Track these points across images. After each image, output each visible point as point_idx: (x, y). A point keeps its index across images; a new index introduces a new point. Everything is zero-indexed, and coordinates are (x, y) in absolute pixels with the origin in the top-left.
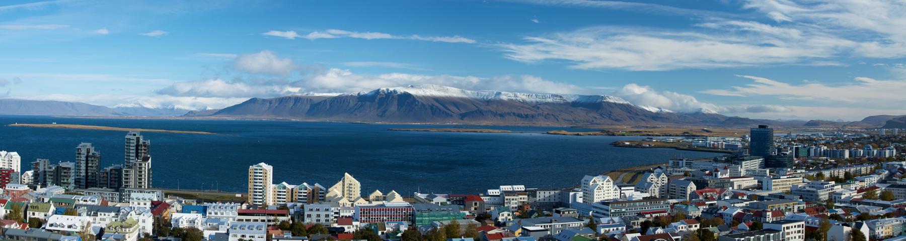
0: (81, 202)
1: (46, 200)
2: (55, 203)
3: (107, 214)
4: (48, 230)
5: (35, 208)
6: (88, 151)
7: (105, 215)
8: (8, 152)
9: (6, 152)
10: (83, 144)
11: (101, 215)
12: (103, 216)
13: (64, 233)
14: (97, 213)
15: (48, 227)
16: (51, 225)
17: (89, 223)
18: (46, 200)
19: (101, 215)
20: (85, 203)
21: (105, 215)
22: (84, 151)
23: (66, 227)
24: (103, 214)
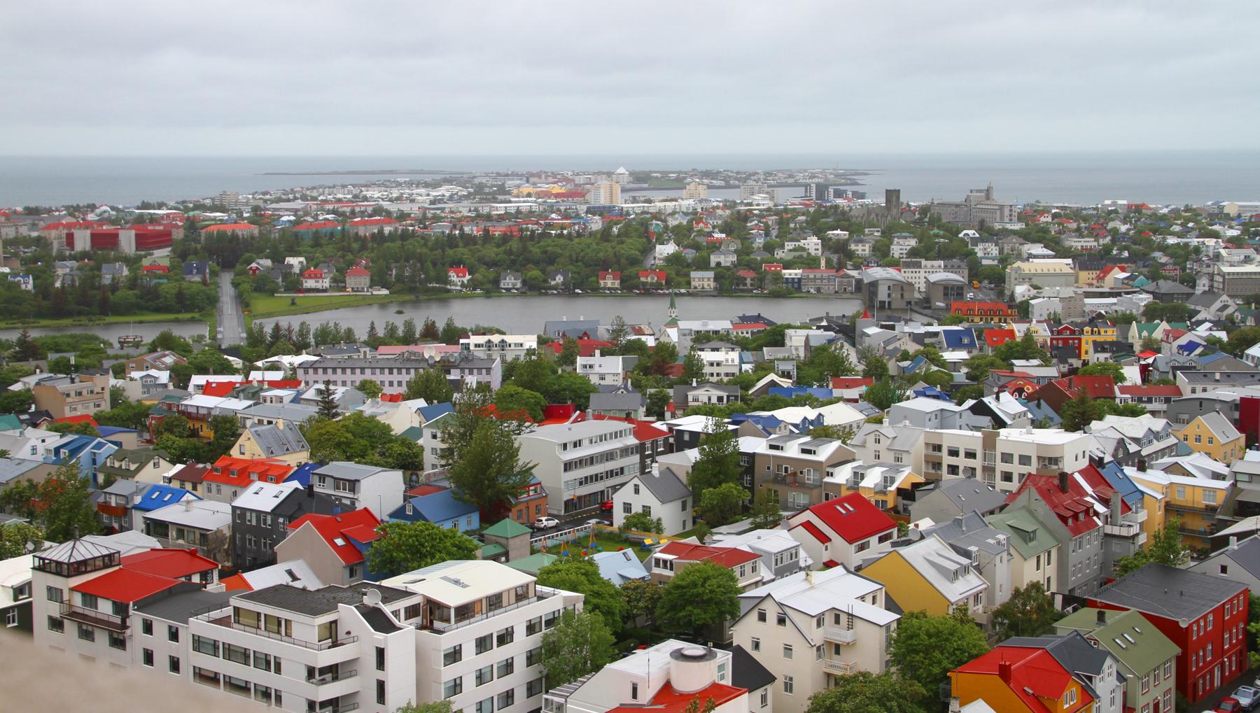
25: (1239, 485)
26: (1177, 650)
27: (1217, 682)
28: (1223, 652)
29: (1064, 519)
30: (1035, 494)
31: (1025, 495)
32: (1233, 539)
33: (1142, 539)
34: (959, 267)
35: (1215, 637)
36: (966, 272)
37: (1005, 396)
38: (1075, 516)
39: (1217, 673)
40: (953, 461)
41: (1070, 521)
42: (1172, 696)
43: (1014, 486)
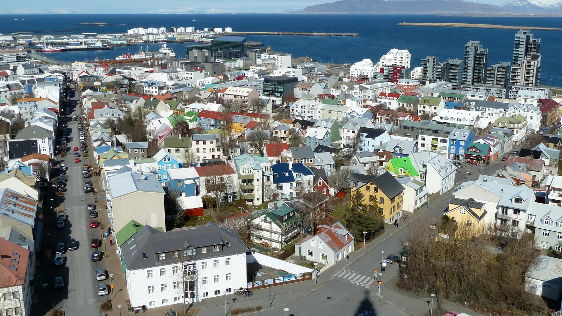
0: (470, 98)
1: (436, 95)
2: (445, 97)
3: (495, 109)
4: (439, 123)
5: (426, 102)
6: (476, 49)
7: (493, 110)
8: (399, 49)
9: (397, 50)
10: (471, 42)
11: (489, 110)
12: (490, 111)
13: (454, 126)
14: (485, 109)
15: (438, 120)
16: (442, 118)
17: (478, 118)
18: (436, 95)
19: (489, 110)
20: (473, 98)
21: (493, 110)
22: (472, 49)
23: (456, 120)
24: (491, 109)
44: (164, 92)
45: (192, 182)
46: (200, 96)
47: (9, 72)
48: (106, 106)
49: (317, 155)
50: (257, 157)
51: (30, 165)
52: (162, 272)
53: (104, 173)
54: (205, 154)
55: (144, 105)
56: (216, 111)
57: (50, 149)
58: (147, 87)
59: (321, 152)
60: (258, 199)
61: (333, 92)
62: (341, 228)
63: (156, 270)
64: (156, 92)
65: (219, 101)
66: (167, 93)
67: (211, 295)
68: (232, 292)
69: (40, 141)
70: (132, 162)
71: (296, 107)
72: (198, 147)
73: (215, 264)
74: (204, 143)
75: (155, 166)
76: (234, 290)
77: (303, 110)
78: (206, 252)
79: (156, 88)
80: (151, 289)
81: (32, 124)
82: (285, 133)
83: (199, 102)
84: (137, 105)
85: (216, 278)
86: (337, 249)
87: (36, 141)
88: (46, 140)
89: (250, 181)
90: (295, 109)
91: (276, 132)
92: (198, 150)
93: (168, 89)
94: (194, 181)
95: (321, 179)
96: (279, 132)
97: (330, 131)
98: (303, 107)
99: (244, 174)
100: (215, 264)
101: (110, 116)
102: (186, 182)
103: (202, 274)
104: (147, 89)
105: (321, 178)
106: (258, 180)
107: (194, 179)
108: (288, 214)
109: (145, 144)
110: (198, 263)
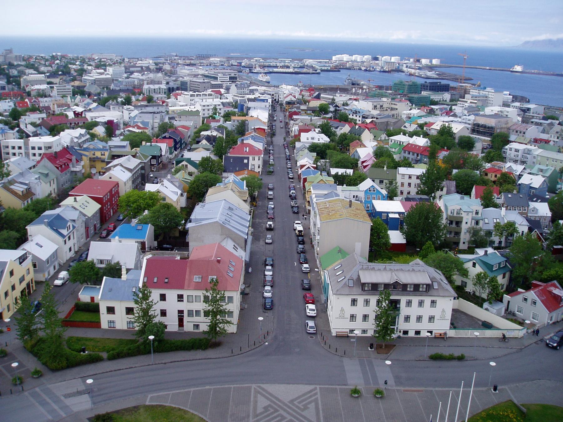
25: (112, 149)
26: (100, 206)
27: (112, 214)
28: (113, 204)
29: (58, 168)
30: (47, 160)
31: (43, 160)
32: (112, 168)
33: (83, 171)
34: (3, 79)
35: (110, 200)
36: (6, 80)
37: (516, 67)
38: (61, 166)
39: (112, 211)
40: (34, 151)
41: (60, 168)
42: (99, 222)
43: (38, 158)
44: (368, 121)
45: (397, 216)
46: (405, 129)
47: (222, 91)
48: (313, 130)
49: (532, 205)
50: (466, 198)
51: (243, 179)
52: (367, 302)
53: (311, 197)
54: (409, 189)
55: (349, 132)
56: (422, 145)
57: (259, 167)
58: (351, 115)
59: (536, 201)
60: (464, 243)
61: (551, 137)
62: (557, 287)
63: (361, 300)
64: (359, 121)
65: (426, 135)
66: (372, 122)
67: (411, 334)
68: (433, 336)
69: (251, 158)
70: (339, 187)
71: (508, 149)
72: (403, 181)
73: (421, 303)
74: (410, 177)
75: (362, 195)
76: (435, 333)
77: (517, 153)
78: (412, 290)
79: (360, 117)
80: (353, 317)
81: (245, 142)
82: (496, 176)
83: (404, 134)
84: (342, 131)
85: (419, 319)
86: (551, 309)
87: (248, 158)
88: (257, 158)
89: (458, 223)
90: (508, 152)
91: (486, 175)
92: (402, 184)
93: (372, 118)
94: (399, 216)
95: (536, 231)
96: (489, 175)
97: (547, 181)
98: (517, 151)
99: (452, 215)
100: (421, 303)
101: (316, 141)
102: (391, 216)
103: (404, 310)
104: (350, 117)
105: (536, 230)
106: (466, 223)
107: (399, 213)
108: (500, 264)
109: (350, 172)
110: (403, 300)
